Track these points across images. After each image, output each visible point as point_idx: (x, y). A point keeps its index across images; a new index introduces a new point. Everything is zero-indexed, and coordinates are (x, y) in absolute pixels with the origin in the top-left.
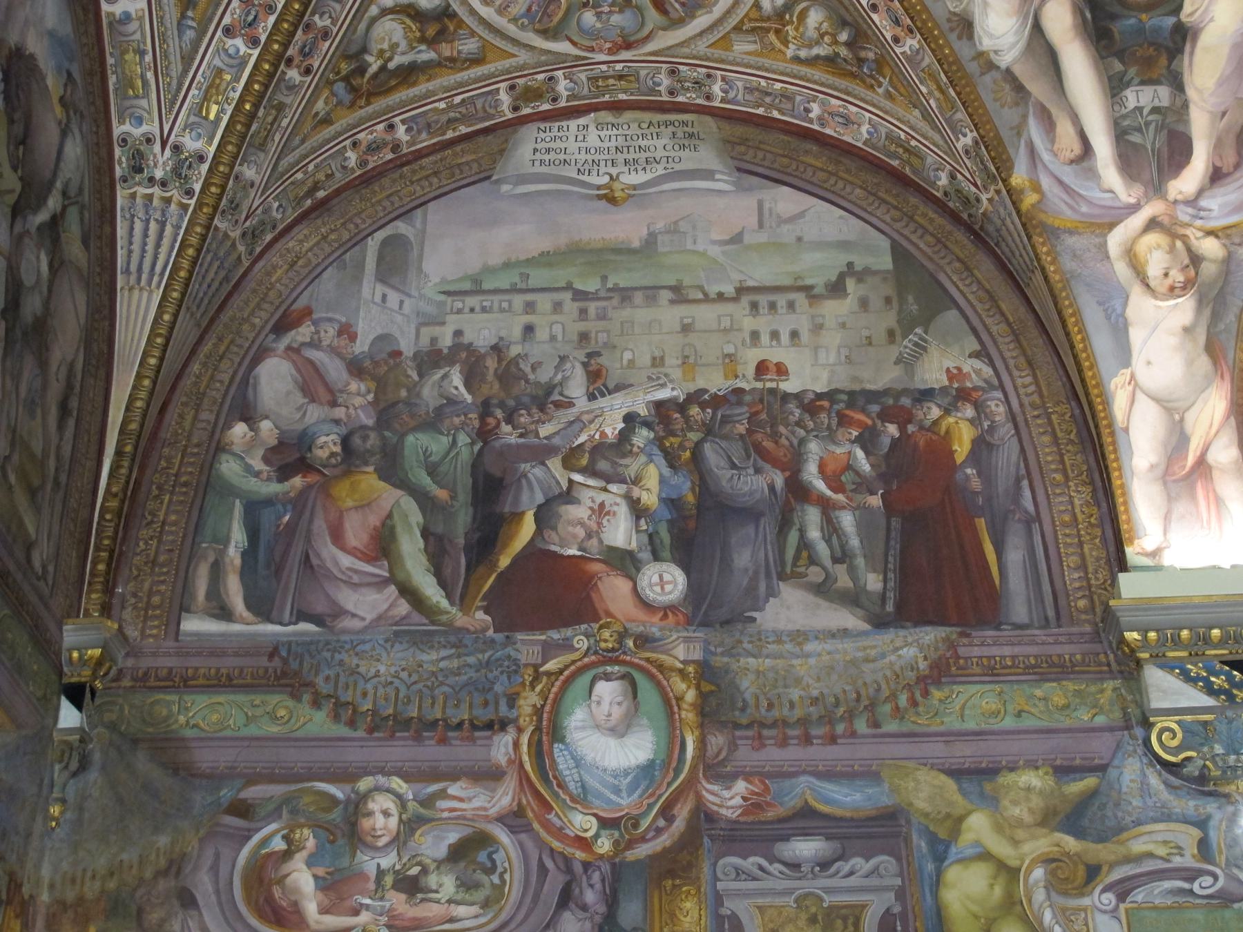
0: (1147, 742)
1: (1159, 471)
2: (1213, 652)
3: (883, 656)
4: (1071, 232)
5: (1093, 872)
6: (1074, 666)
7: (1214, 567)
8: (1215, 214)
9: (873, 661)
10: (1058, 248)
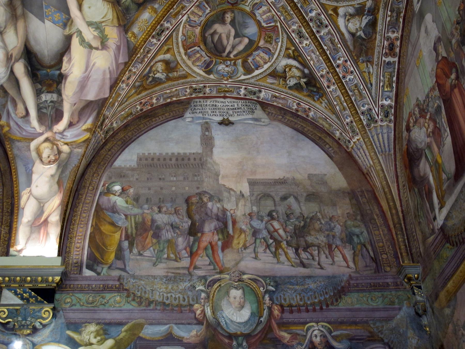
1: (30, 223)
2: (27, 285)
4: (18, 141)
7: (39, 256)
8: (68, 137)
10: (13, 146)
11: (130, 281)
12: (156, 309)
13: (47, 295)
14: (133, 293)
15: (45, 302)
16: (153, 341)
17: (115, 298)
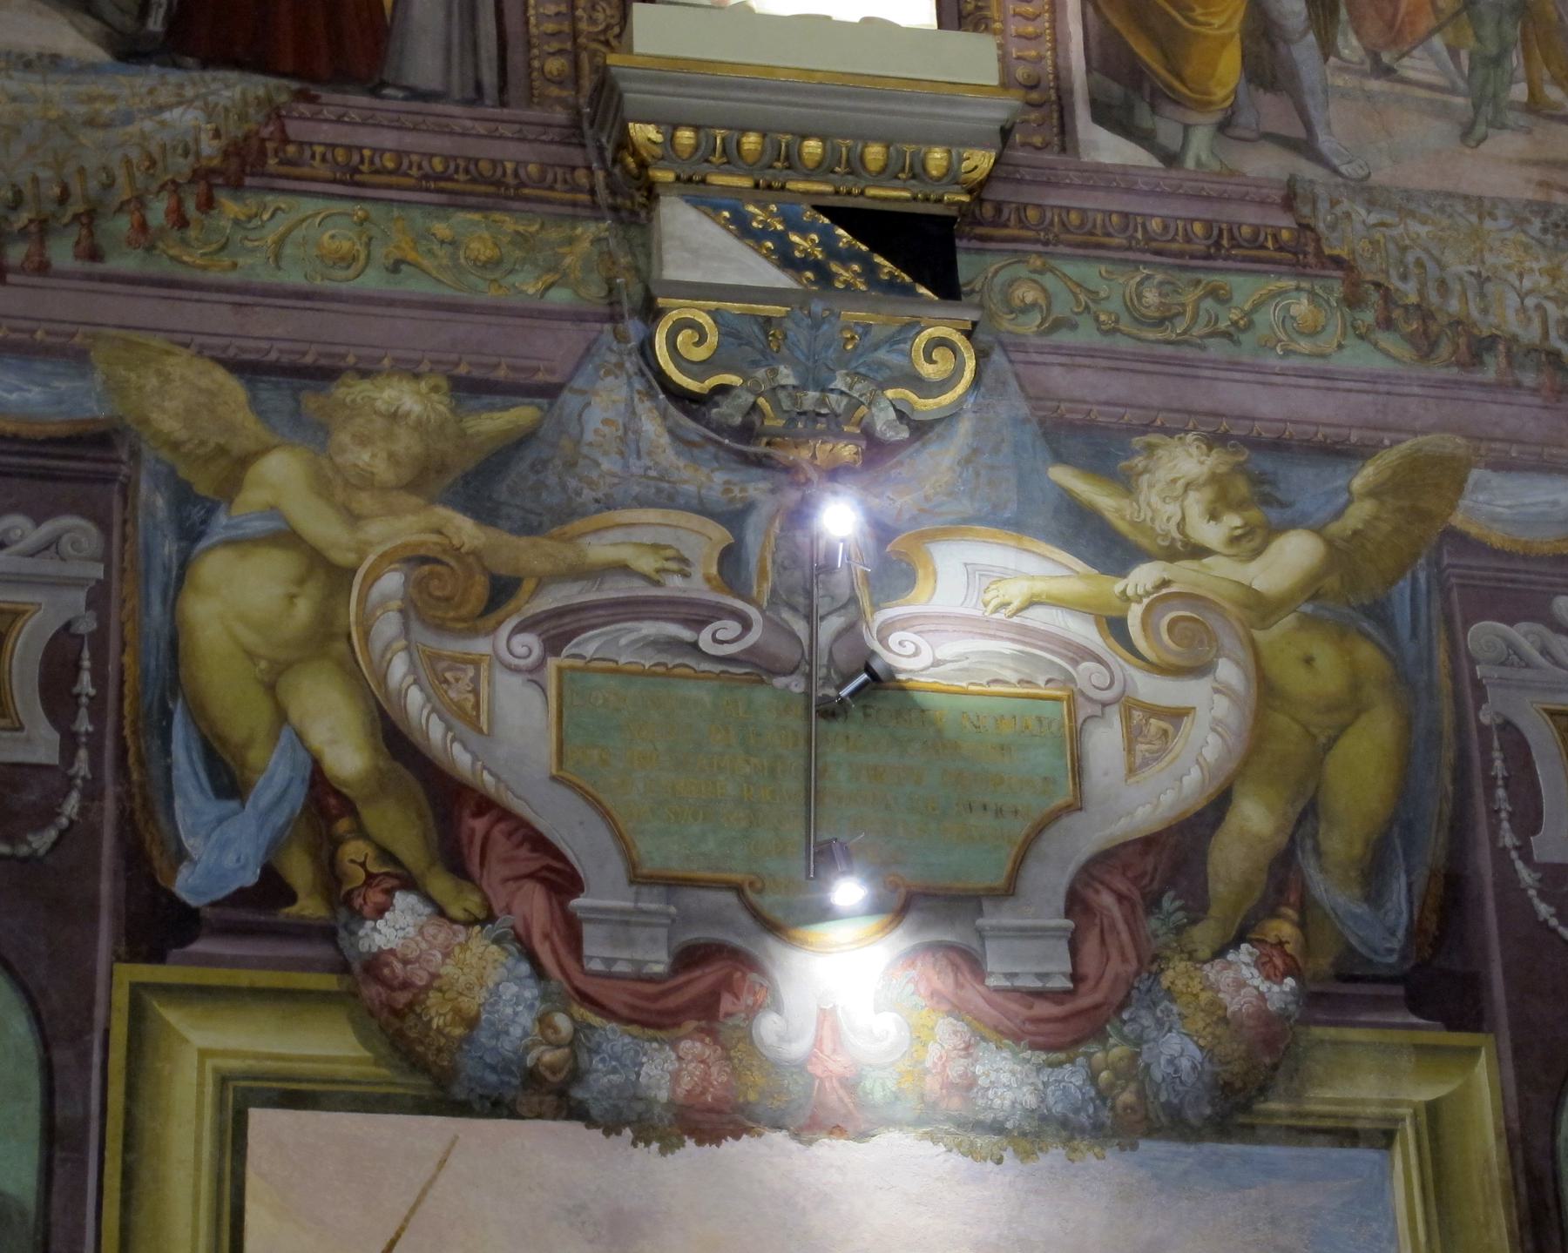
0: (646, 349)
2: (801, 186)
3: (128, 118)
5: (502, 590)
6: (523, 185)
9: (107, 126)
11: (1348, 215)
12: (1518, 385)
13: (920, 247)
14: (1378, 285)
15: (922, 290)
16: (1525, 558)
17: (1289, 305)
